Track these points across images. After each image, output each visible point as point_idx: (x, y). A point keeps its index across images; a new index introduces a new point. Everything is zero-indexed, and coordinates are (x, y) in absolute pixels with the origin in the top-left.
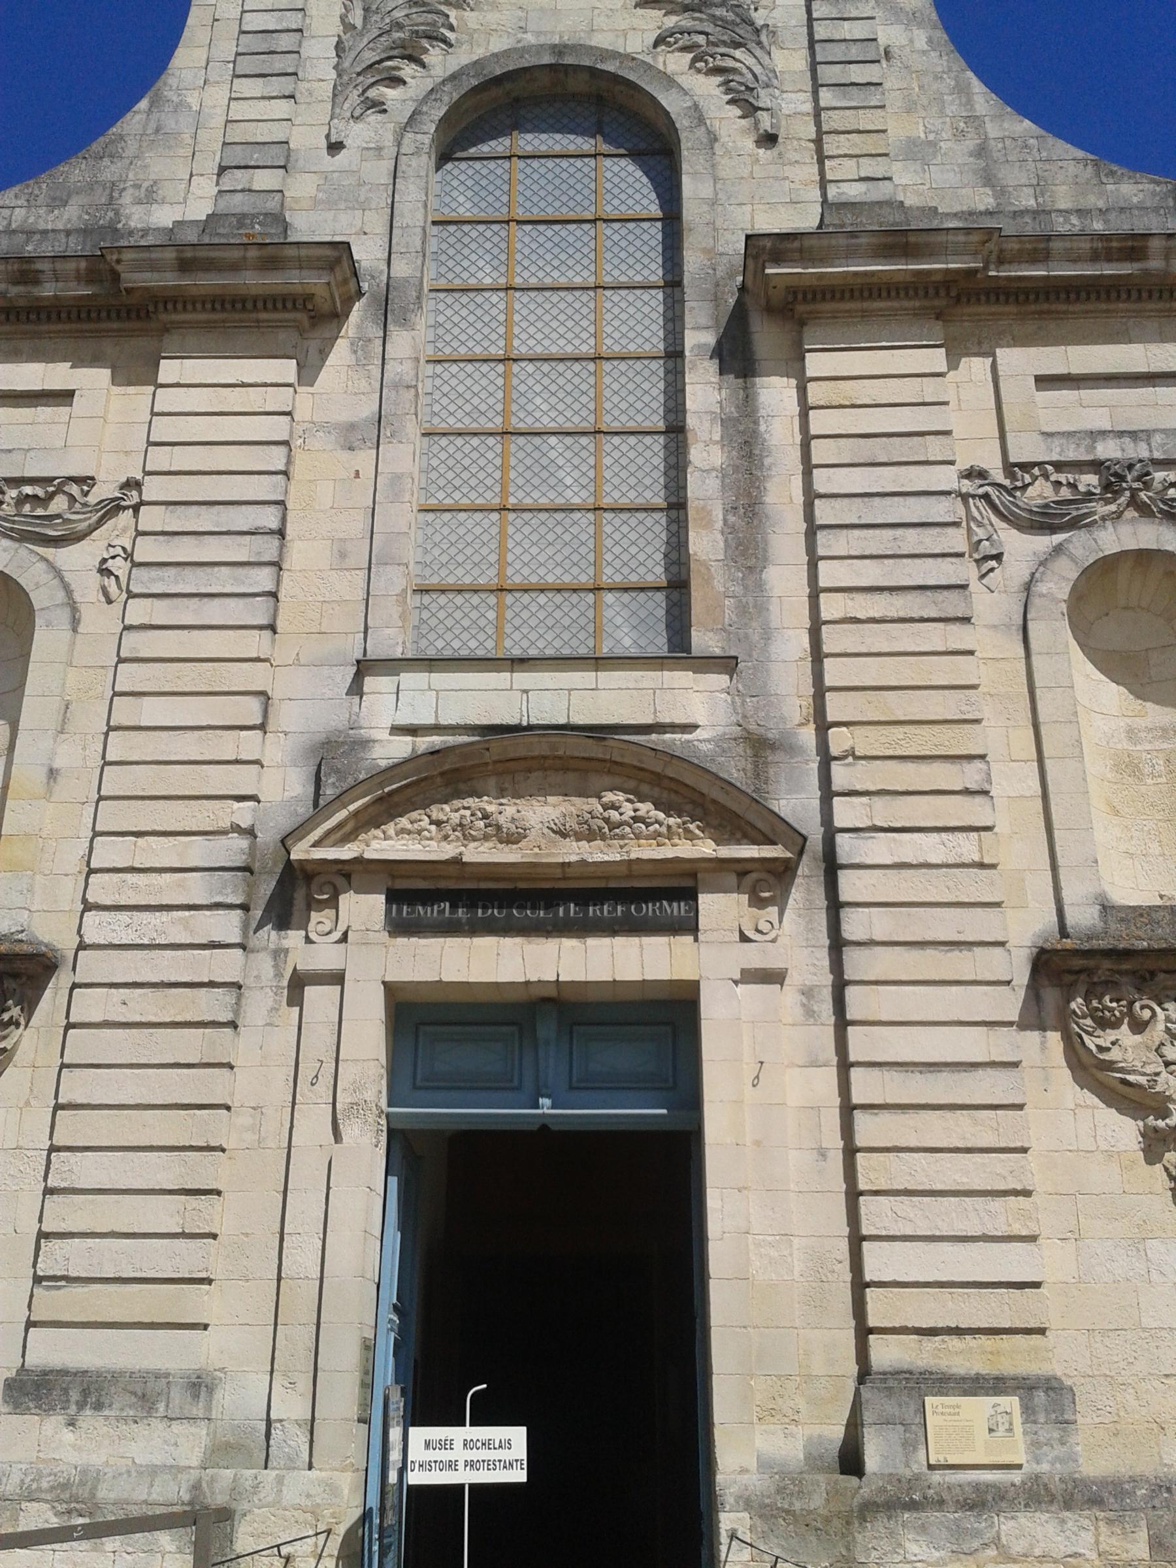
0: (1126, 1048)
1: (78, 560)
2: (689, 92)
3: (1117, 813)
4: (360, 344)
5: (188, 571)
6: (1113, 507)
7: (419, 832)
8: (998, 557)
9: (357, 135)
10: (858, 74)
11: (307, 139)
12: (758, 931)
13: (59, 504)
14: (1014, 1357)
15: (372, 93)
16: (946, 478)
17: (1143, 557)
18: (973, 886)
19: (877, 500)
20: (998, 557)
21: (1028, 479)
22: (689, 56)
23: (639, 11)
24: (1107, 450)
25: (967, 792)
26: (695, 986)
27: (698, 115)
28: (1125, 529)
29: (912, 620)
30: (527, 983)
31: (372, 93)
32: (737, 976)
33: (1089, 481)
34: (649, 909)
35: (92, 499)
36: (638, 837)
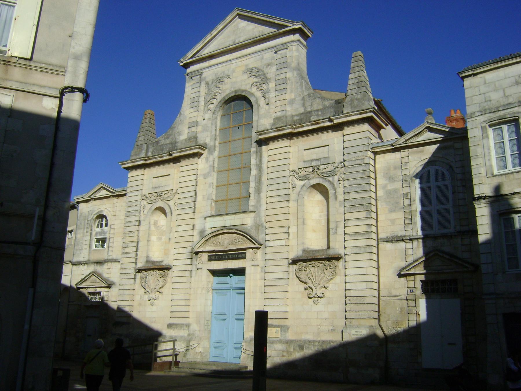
0: (303, 276)
1: (171, 203)
2: (255, 95)
4: (207, 159)
10: (282, 87)
11: (200, 119)
13: (169, 194)
14: (282, 323)
15: (209, 107)
16: (288, 173)
22: (256, 87)
24: (314, 164)
28: (314, 180)
33: (311, 169)
34: (240, 256)
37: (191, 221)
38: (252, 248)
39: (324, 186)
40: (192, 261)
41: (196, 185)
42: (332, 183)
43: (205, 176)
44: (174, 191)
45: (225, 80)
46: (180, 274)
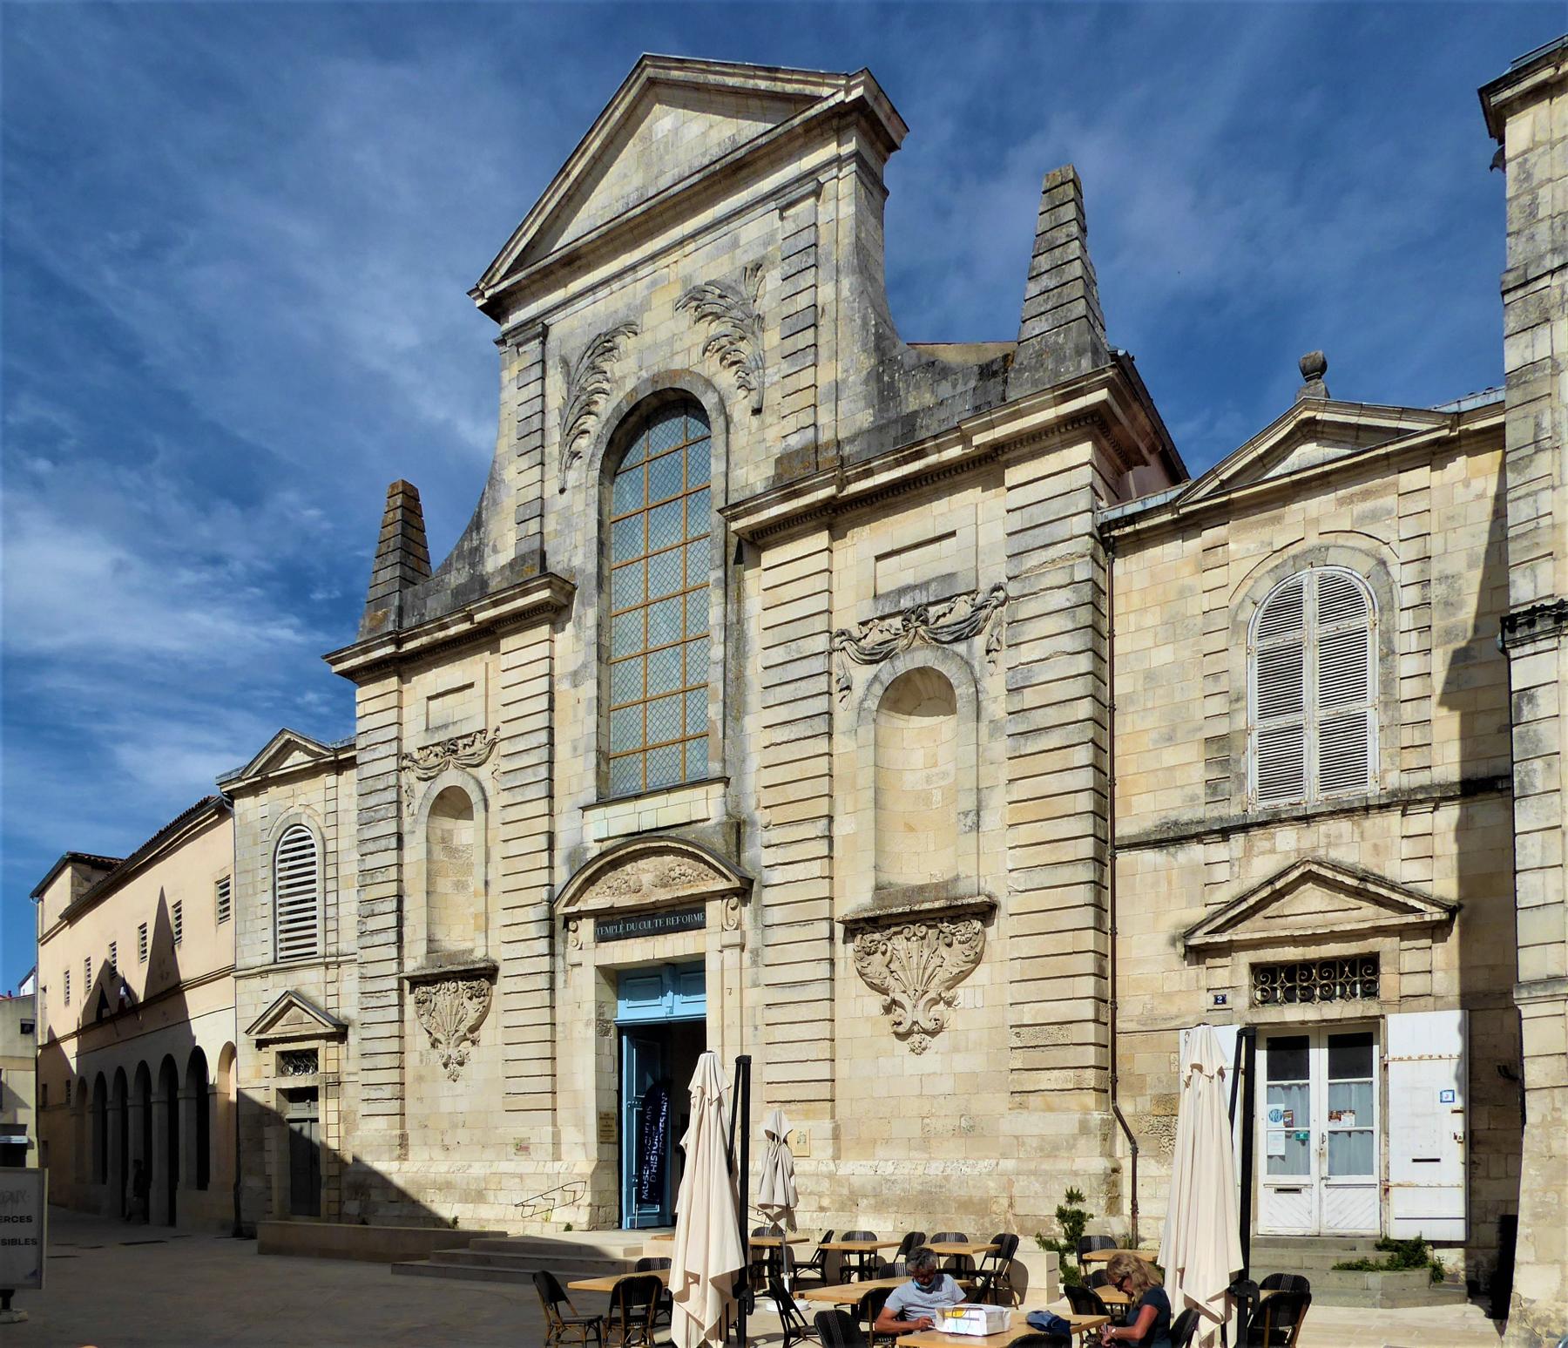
17: (923, 671)
20: (848, 688)
21: (865, 630)
28: (908, 657)
33: (897, 622)
37: (543, 824)
39: (940, 676)
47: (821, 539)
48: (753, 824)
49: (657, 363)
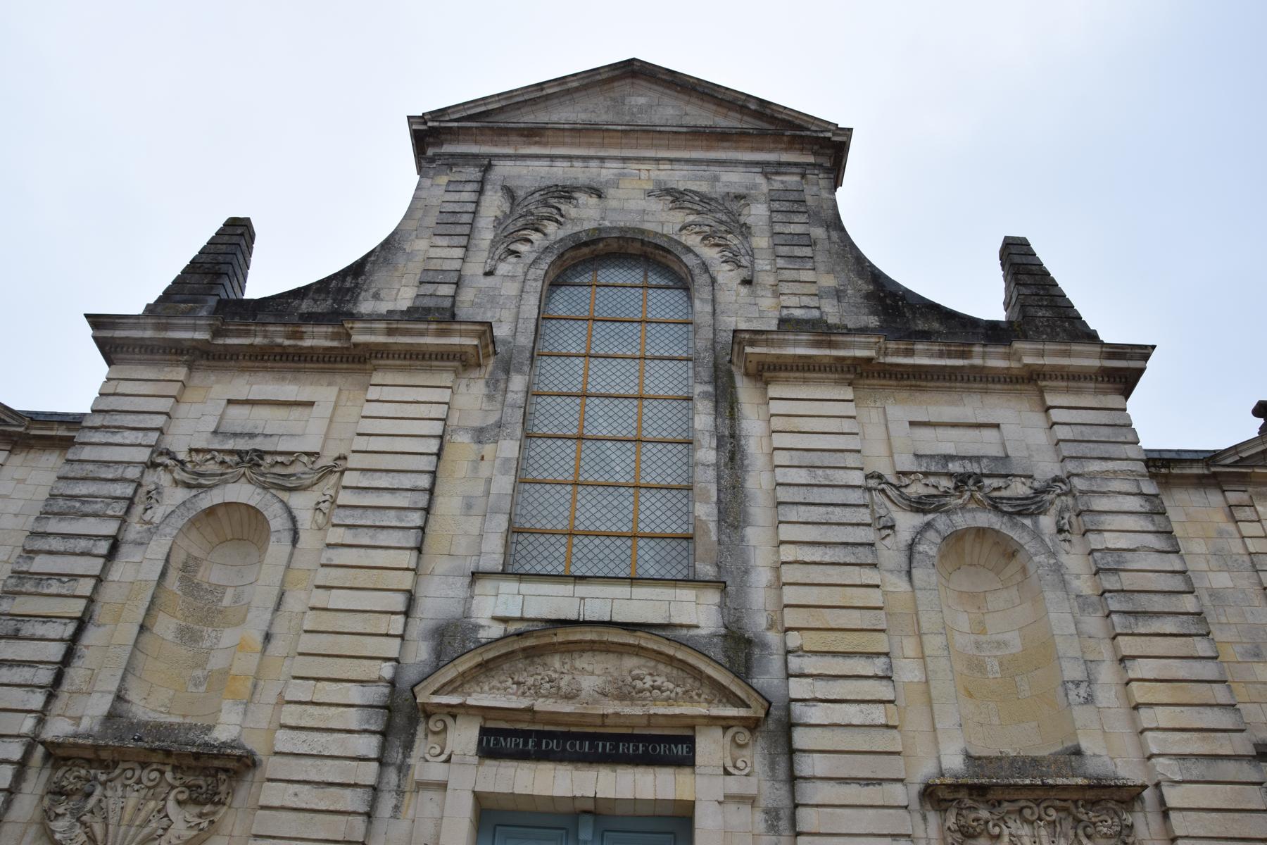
1: (302, 503)
3: (971, 696)
5: (369, 512)
6: (960, 501)
7: (505, 689)
8: (892, 527)
9: (503, 268)
12: (735, 766)
13: (297, 469)
16: (857, 478)
17: (981, 532)
18: (881, 741)
19: (815, 489)
23: (672, 213)
24: (954, 467)
25: (876, 677)
26: (691, 805)
27: (705, 267)
28: (968, 516)
29: (839, 564)
30: (574, 798)
31: (512, 247)
32: (722, 799)
34: (662, 749)
35: (317, 466)
36: (655, 700)
37: (406, 581)
38: (725, 724)
40: (383, 748)
41: (438, 455)
42: (1037, 534)
43: (480, 435)
44: (325, 461)
45: (582, 198)
46: (308, 797)
47: (848, 393)
48: (764, 646)
49: (622, 221)
